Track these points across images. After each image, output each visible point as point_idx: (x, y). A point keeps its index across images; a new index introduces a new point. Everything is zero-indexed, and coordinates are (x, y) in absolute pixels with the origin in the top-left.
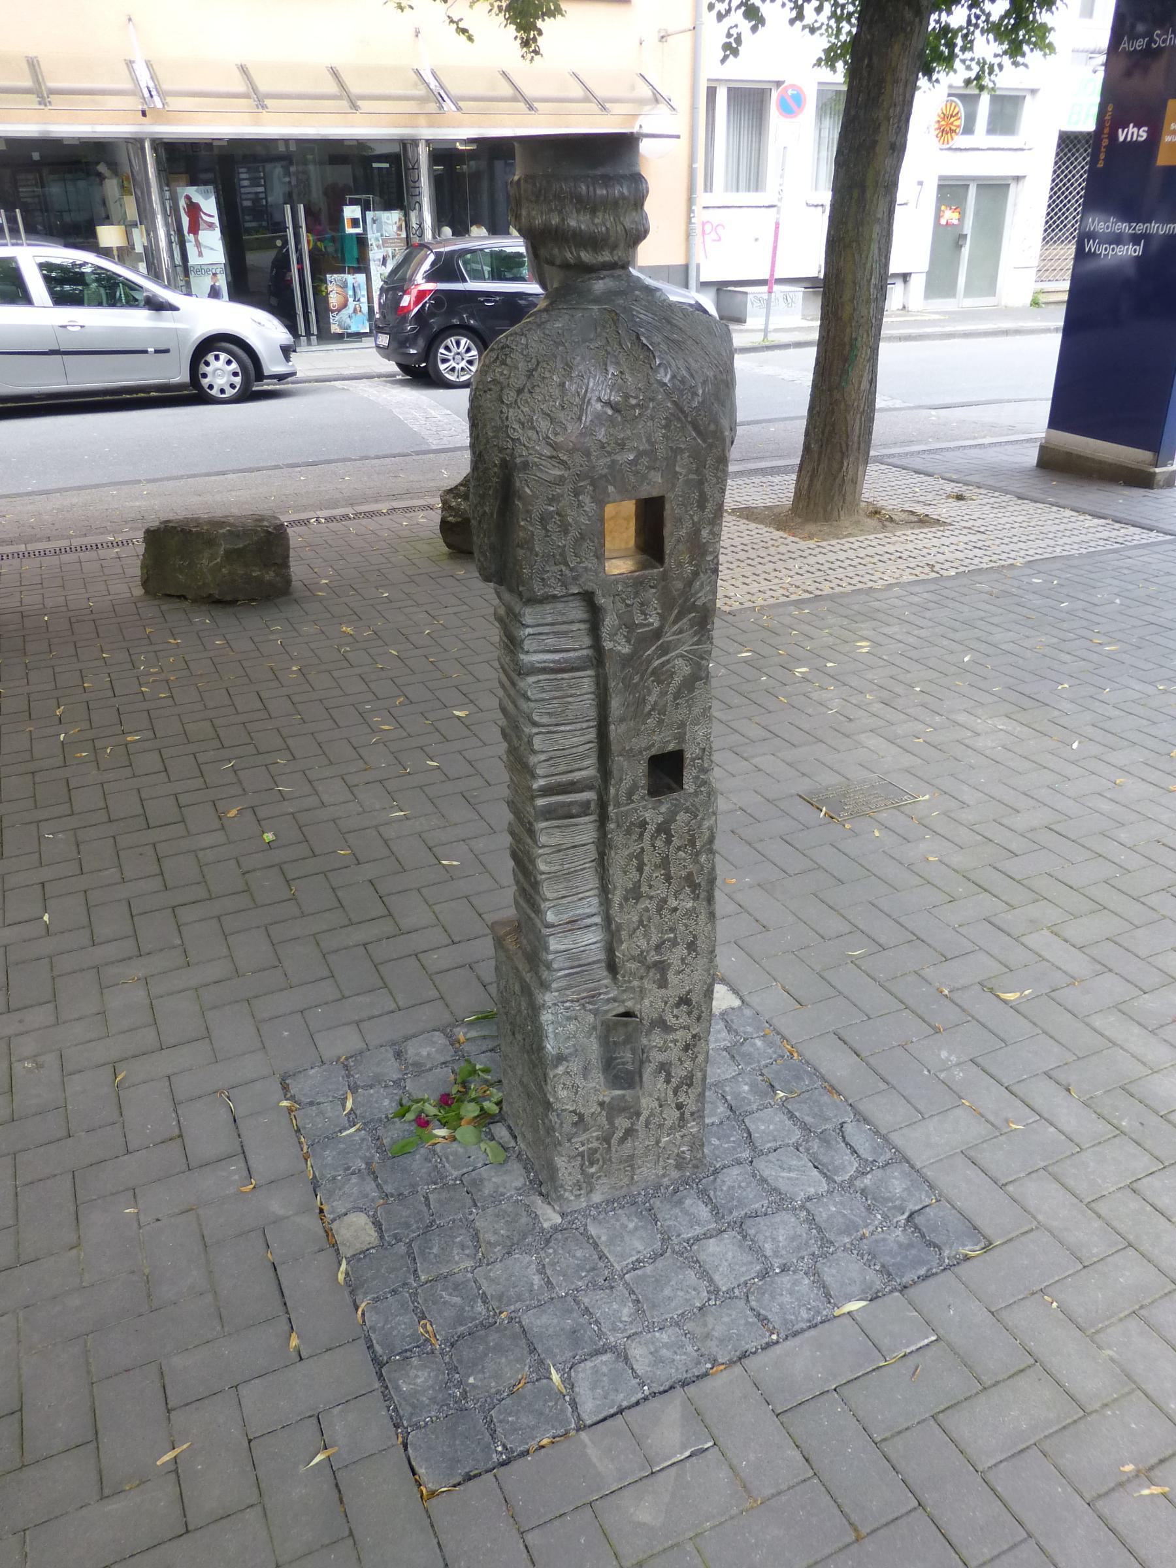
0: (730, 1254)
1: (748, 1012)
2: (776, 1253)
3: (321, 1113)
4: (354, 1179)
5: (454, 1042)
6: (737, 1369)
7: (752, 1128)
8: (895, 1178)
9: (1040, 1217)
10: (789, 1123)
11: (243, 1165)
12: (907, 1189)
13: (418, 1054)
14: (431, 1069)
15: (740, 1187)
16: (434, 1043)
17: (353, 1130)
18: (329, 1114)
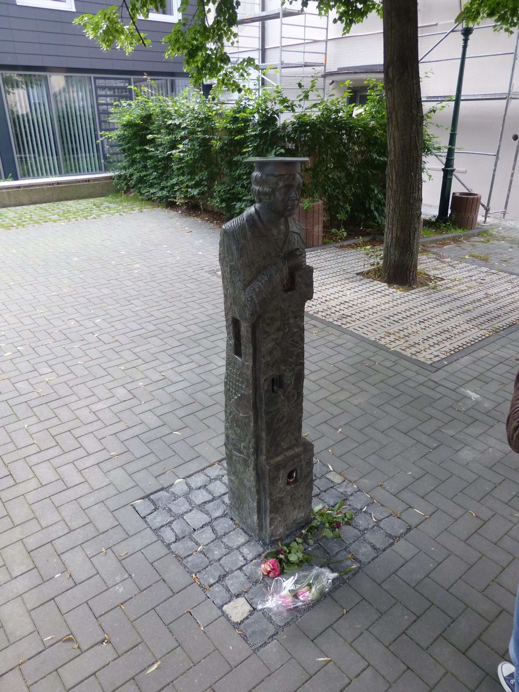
0: (217, 489)
1: (218, 601)
2: (202, 492)
3: (382, 514)
4: (349, 493)
5: (355, 559)
6: (212, 462)
7: (212, 534)
8: (158, 522)
9: (111, 515)
10: (198, 539)
11: (390, 491)
12: (155, 519)
13: (365, 547)
14: (354, 542)
15: (215, 510)
16: (363, 555)
17: (364, 510)
18: (378, 514)
